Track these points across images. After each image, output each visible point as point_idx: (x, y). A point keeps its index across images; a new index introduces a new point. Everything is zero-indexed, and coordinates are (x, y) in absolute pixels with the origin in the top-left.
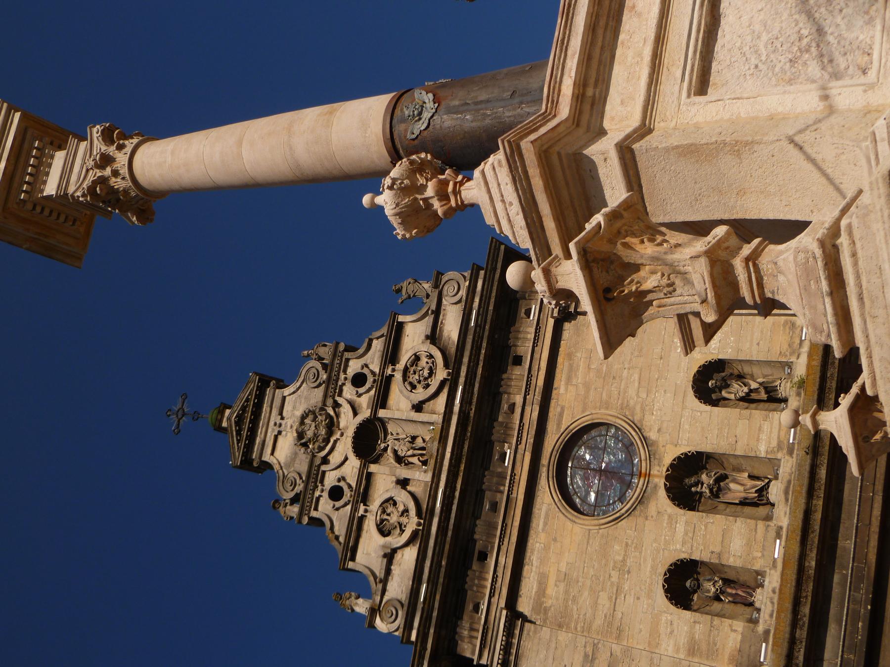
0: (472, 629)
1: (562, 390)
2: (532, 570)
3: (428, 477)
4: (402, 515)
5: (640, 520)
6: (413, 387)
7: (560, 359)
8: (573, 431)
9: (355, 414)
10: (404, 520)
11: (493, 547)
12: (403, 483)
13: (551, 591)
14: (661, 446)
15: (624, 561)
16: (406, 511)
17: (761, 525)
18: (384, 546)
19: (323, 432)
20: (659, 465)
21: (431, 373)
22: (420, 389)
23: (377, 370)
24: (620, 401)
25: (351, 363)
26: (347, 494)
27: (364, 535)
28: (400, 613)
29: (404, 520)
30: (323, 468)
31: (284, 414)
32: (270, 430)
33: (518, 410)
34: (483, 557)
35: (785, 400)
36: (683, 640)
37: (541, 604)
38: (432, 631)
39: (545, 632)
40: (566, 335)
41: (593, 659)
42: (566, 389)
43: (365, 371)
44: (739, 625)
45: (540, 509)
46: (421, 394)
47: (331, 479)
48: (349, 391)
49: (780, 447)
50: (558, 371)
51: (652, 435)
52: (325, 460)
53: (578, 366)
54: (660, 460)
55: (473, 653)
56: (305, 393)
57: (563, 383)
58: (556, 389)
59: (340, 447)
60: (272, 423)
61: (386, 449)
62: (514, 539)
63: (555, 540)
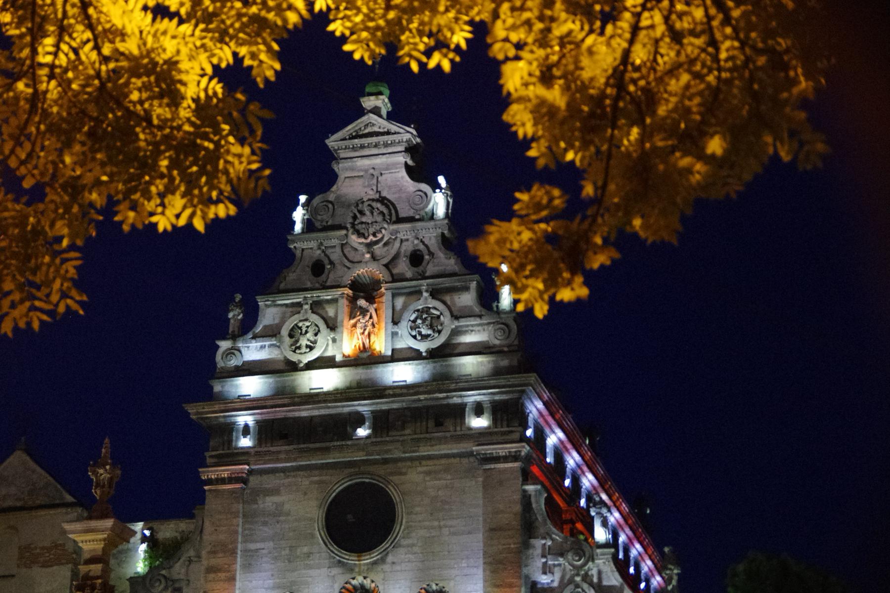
1: (420, 469)
2: (282, 480)
8: (387, 489)
10: (304, 350)
14: (382, 567)
15: (298, 557)
20: (368, 569)
24: (413, 524)
37: (258, 495)
42: (421, 473)
45: (326, 475)
51: (390, 558)
53: (440, 479)
57: (425, 468)
58: (420, 463)
63: (305, 494)
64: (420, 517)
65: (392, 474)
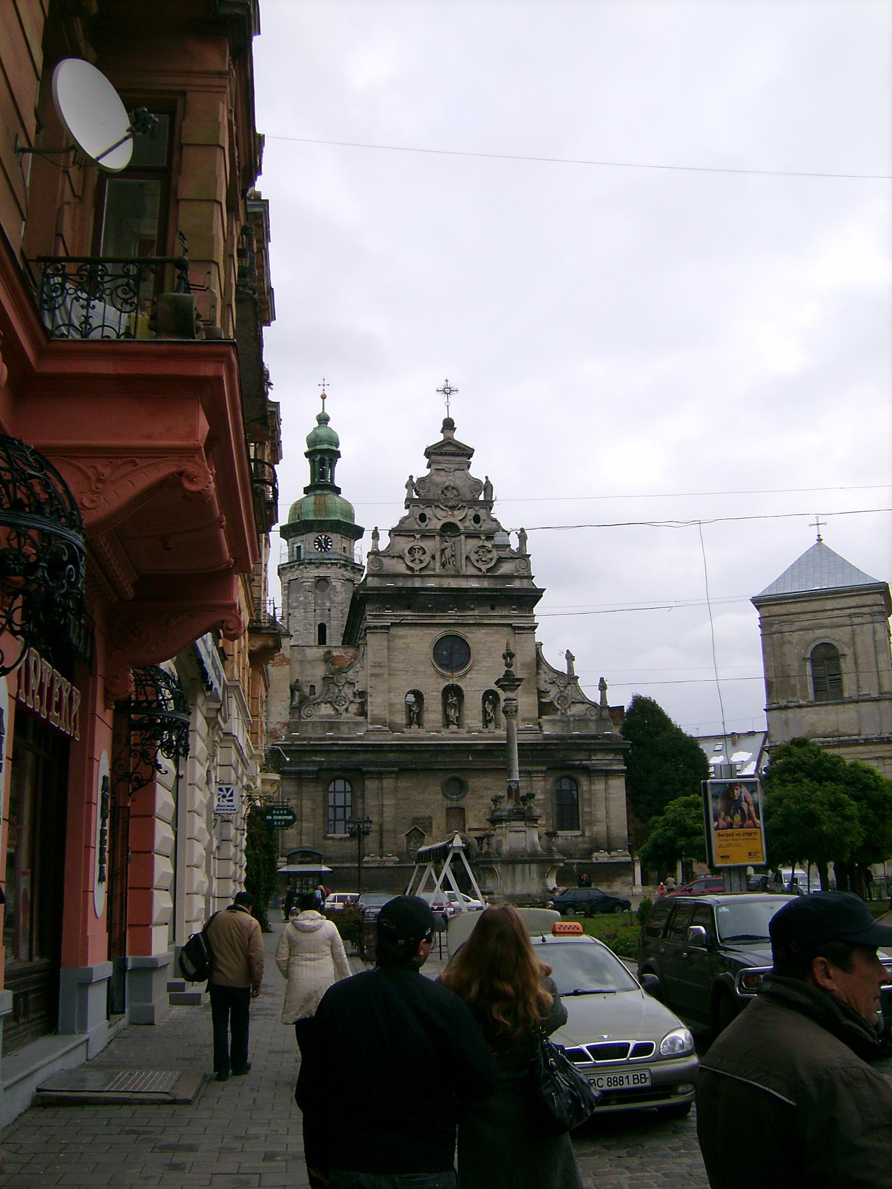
0: (379, 608)
1: (482, 631)
3: (438, 570)
4: (420, 560)
5: (435, 676)
6: (477, 553)
7: (495, 628)
9: (460, 520)
10: (417, 561)
11: (413, 612)
12: (433, 557)
13: (402, 641)
16: (421, 561)
17: (441, 725)
18: (404, 554)
19: (450, 504)
21: (483, 561)
22: (476, 557)
23: (482, 528)
25: (485, 510)
26: (423, 525)
27: (407, 539)
28: (378, 568)
29: (417, 561)
30: (433, 506)
31: (457, 472)
32: (446, 465)
33: (471, 613)
34: (409, 608)
35: (487, 727)
36: (394, 701)
38: (376, 592)
39: (385, 643)
40: (506, 629)
41: (380, 666)
43: (481, 521)
44: (404, 721)
46: (473, 557)
47: (428, 512)
48: (471, 513)
49: (470, 728)
50: (490, 628)
51: (468, 676)
52: (436, 506)
54: (457, 681)
55: (370, 611)
56: (468, 484)
59: (444, 514)
60: (450, 466)
61: (447, 542)
62: (419, 622)
64: (483, 656)
65: (467, 632)
